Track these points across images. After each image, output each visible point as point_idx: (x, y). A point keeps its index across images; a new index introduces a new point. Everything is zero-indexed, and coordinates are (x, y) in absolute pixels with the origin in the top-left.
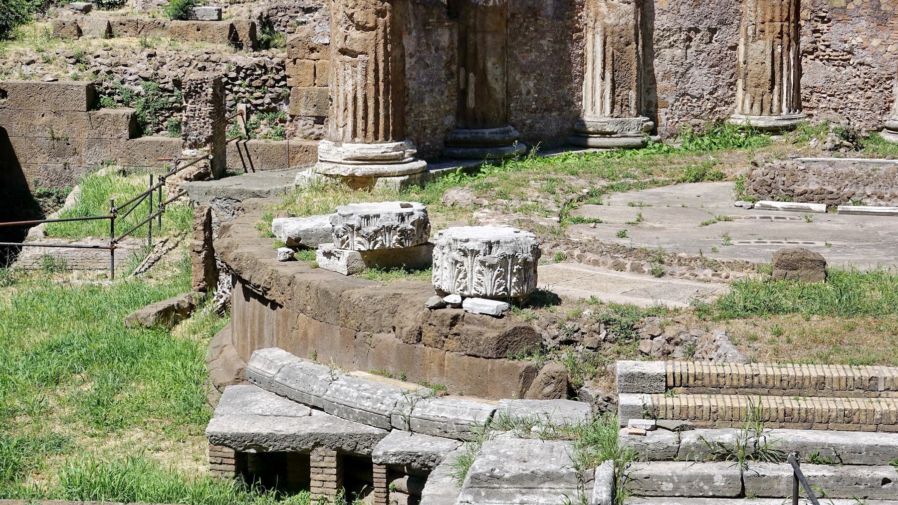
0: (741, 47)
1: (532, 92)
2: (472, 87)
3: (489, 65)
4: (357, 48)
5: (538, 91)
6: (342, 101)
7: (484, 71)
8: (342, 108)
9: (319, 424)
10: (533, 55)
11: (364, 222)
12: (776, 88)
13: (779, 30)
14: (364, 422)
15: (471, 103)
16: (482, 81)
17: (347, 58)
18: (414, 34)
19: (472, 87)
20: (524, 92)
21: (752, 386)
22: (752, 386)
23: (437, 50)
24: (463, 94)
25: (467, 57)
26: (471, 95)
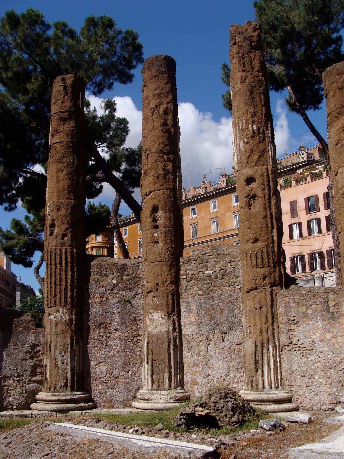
10: (104, 351)
12: (260, 371)
13: (259, 331)
20: (98, 373)
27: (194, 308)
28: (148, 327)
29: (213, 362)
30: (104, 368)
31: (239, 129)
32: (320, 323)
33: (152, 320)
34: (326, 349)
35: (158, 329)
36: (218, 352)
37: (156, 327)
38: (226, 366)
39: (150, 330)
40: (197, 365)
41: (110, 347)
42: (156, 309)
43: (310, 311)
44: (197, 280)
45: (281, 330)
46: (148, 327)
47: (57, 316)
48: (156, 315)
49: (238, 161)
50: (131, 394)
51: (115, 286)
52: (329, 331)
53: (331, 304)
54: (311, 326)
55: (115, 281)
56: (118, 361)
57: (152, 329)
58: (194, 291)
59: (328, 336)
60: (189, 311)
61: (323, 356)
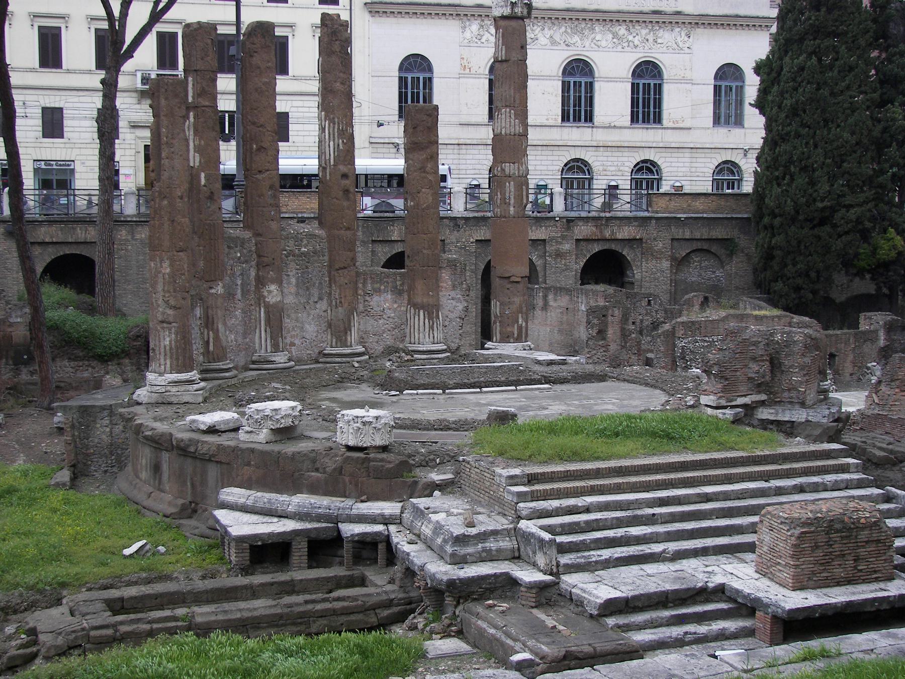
0: (329, 311)
2: (211, 340)
3: (220, 326)
4: (171, 319)
5: (236, 341)
6: (162, 350)
7: (218, 330)
8: (163, 354)
9: (289, 525)
11: (274, 413)
14: (319, 521)
15: (211, 348)
16: (217, 338)
17: (165, 325)
21: (567, 476)
22: (567, 476)
24: (208, 342)
25: (208, 323)
26: (211, 344)
27: (293, 280)
32: (389, 296)
33: (270, 292)
35: (274, 300)
37: (273, 297)
42: (273, 283)
43: (382, 287)
48: (273, 287)
50: (249, 359)
51: (239, 258)
53: (398, 283)
54: (382, 298)
55: (239, 255)
56: (240, 329)
58: (292, 265)
59: (395, 306)
60: (289, 283)
61: (391, 320)
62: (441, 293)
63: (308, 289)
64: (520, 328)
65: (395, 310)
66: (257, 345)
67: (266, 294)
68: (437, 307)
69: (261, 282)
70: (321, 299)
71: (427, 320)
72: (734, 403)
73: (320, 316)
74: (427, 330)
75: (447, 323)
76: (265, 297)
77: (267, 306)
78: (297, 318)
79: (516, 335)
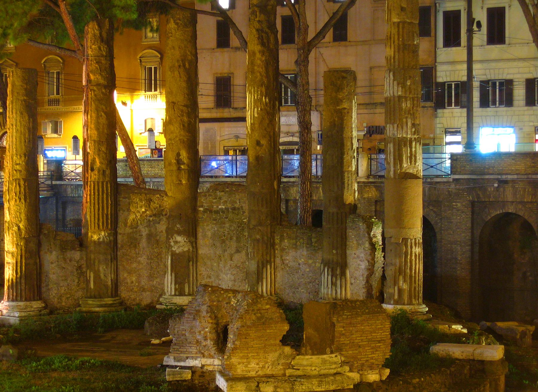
1: (134, 282)
2: (92, 279)
10: (134, 265)
16: (97, 277)
18: (54, 253)
19: (92, 279)
23: (70, 261)
24: (88, 282)
28: (172, 247)
29: (223, 276)
30: (134, 279)
31: (254, 97)
32: (305, 253)
33: (176, 242)
34: (308, 270)
36: (227, 268)
37: (179, 247)
38: (233, 278)
39: (173, 249)
40: (210, 277)
41: (139, 262)
42: (179, 233)
44: (211, 211)
45: (277, 255)
46: (172, 247)
47: (100, 238)
48: (179, 238)
49: (251, 124)
52: (311, 259)
56: (145, 273)
57: (176, 249)
59: (310, 262)
60: (205, 236)
62: (348, 252)
63: (223, 242)
64: (400, 291)
65: (310, 266)
66: (166, 288)
67: (172, 244)
68: (344, 266)
69: (170, 232)
70: (238, 251)
71: (330, 277)
72: (182, 364)
73: (237, 267)
74: (330, 286)
75: (353, 281)
76: (171, 246)
77: (173, 254)
78: (212, 265)
79: (396, 297)
